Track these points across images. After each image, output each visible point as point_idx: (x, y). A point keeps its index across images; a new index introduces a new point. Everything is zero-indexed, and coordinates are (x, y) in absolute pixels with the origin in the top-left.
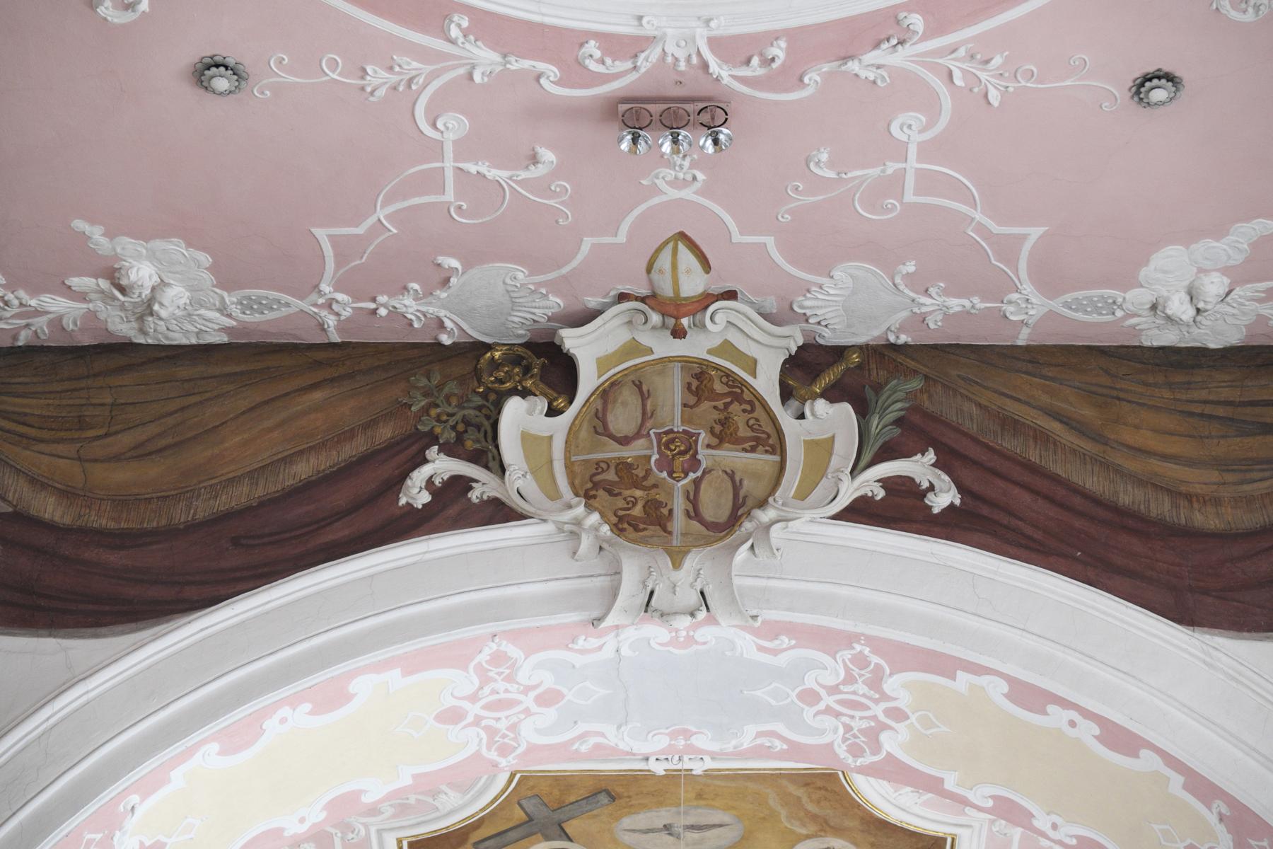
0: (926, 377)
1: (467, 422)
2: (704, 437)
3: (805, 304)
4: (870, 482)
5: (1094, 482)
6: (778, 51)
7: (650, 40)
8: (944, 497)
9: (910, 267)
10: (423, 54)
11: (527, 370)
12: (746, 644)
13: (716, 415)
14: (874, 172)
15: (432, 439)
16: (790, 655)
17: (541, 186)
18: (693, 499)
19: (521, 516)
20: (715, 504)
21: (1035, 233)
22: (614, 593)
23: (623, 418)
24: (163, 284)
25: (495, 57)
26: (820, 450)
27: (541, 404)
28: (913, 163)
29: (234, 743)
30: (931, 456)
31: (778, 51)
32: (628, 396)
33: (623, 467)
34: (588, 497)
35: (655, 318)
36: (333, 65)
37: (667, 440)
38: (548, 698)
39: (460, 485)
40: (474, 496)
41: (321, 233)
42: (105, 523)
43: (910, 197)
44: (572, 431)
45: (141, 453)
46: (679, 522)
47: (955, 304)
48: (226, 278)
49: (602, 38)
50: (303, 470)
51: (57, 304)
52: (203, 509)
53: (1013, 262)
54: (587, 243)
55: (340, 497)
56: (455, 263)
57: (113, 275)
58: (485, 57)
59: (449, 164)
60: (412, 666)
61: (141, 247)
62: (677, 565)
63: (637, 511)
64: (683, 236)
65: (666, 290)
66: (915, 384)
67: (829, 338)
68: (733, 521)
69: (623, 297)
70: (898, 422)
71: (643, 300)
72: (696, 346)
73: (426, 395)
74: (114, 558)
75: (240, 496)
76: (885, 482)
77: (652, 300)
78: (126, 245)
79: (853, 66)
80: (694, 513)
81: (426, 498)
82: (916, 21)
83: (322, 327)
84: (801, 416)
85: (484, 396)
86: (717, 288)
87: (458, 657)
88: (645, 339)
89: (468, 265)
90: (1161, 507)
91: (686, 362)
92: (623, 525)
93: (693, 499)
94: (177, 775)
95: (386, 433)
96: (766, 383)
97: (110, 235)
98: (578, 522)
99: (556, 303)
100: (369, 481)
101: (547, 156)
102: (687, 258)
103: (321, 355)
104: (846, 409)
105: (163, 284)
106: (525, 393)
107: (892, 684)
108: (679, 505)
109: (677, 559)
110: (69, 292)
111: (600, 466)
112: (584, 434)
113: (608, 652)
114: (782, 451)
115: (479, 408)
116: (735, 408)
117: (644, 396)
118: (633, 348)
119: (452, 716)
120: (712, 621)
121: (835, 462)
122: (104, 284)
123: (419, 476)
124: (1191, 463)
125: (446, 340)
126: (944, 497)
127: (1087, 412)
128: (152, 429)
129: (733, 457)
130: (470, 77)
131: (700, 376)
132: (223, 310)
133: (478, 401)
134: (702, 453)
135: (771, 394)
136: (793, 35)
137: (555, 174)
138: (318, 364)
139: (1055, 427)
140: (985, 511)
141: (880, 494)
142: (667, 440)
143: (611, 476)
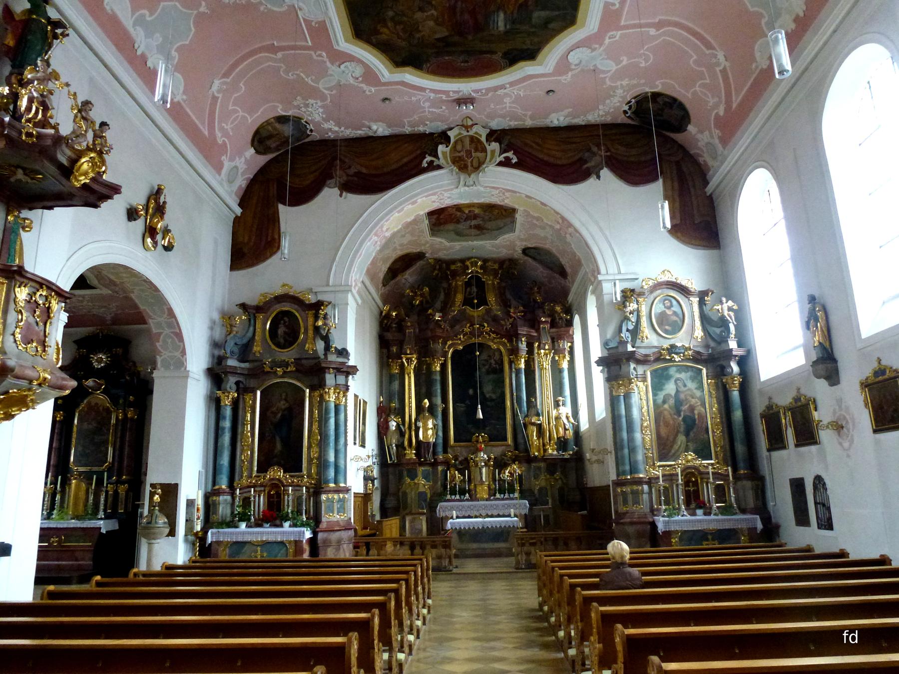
3: (489, 124)
4: (502, 158)
5: (541, 156)
6: (484, 91)
7: (461, 91)
8: (515, 160)
10: (421, 95)
12: (482, 189)
14: (501, 106)
15: (425, 153)
16: (488, 190)
17: (443, 111)
19: (442, 168)
20: (475, 164)
21: (530, 113)
22: (459, 182)
23: (459, 147)
24: (378, 128)
26: (493, 152)
27: (445, 146)
28: (508, 105)
29: (399, 212)
31: (484, 91)
32: (460, 143)
33: (460, 157)
37: (467, 151)
38: (449, 198)
39: (432, 162)
41: (405, 120)
44: (451, 150)
46: (470, 168)
47: (516, 123)
48: (389, 126)
50: (405, 160)
51: (360, 132)
57: (370, 128)
58: (432, 95)
59: (427, 110)
60: (426, 196)
65: (465, 124)
66: (509, 137)
67: (494, 129)
70: (507, 145)
72: (471, 133)
75: (394, 166)
76: (505, 157)
77: (463, 125)
80: (472, 166)
88: (462, 132)
90: (552, 160)
94: (392, 218)
95: (419, 152)
96: (483, 139)
99: (446, 127)
101: (444, 108)
102: (469, 120)
104: (498, 144)
105: (378, 128)
106: (441, 143)
108: (469, 164)
109: (469, 176)
111: (455, 157)
117: (462, 142)
118: (460, 134)
119: (434, 202)
124: (558, 151)
126: (515, 160)
127: (539, 141)
129: (479, 154)
142: (467, 151)
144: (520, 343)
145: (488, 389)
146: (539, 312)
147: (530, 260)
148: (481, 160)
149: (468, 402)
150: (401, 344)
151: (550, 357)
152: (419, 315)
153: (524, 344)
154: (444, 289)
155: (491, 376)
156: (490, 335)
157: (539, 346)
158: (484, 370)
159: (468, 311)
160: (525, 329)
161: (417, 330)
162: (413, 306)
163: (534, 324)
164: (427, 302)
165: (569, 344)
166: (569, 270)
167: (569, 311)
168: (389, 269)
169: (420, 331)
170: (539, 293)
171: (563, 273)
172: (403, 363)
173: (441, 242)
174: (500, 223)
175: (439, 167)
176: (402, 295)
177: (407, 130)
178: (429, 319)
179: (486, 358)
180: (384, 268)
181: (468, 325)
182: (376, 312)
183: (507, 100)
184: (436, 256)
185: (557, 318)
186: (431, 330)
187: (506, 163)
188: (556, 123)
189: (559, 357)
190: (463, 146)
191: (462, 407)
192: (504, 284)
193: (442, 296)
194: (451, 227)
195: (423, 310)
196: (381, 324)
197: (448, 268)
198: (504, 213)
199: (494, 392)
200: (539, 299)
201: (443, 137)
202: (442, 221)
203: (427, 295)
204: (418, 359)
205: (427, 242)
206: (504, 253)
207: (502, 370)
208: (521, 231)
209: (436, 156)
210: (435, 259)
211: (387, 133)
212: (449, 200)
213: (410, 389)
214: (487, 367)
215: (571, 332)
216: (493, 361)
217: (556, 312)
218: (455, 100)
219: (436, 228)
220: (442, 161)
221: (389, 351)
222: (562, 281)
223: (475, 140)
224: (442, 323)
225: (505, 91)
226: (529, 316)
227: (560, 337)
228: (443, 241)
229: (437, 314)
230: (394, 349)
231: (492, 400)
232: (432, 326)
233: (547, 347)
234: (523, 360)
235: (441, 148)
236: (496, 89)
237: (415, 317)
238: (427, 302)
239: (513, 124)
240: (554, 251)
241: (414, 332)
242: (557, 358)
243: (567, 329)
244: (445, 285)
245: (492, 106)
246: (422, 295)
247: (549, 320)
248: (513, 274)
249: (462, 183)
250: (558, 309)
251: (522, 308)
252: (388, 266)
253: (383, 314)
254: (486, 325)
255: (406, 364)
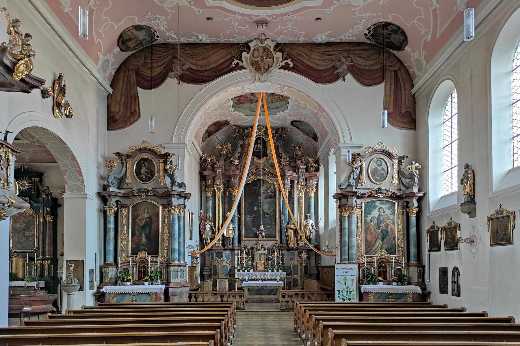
0: (290, 48)
1: (238, 54)
2: (265, 57)
4: (283, 64)
6: (274, 16)
9: (289, 36)
10: (233, 17)
11: (245, 47)
12: (269, 84)
13: (266, 54)
15: (234, 57)
18: (264, 66)
19: (245, 68)
20: (266, 67)
23: (256, 54)
25: (241, 17)
26: (278, 58)
27: (247, 53)
28: (290, 27)
30: (290, 59)
32: (256, 51)
33: (256, 61)
34: (252, 65)
35: (259, 41)
36: (223, 18)
39: (238, 64)
40: (240, 65)
42: (200, 69)
43: (289, 29)
45: (203, 59)
46: (262, 69)
47: (294, 39)
48: (210, 37)
49: (254, 15)
50: (221, 61)
51: (190, 40)
52: (210, 67)
53: (301, 36)
54: (252, 34)
55: (225, 65)
56: (236, 36)
58: (240, 17)
61: (200, 34)
62: (262, 76)
63: (258, 68)
64: (263, 33)
65: (261, 38)
66: (289, 49)
67: (279, 42)
68: (268, 69)
69: (256, 39)
70: (287, 54)
71: (258, 39)
72: (264, 45)
73: (234, 51)
74: (202, 74)
75: (214, 65)
78: (198, 34)
79: (283, 18)
81: (234, 66)
82: (291, 13)
83: (221, 41)
84: (276, 54)
85: (240, 51)
86: (267, 38)
87: (239, 86)
88: (258, 44)
89: (238, 36)
91: (263, 46)
92: (256, 69)
93: (264, 66)
95: (229, 56)
96: (272, 49)
97: (197, 33)
98: (251, 70)
100: (228, 63)
101: (247, 26)
102: (263, 35)
103: (221, 45)
104: (281, 53)
106: (245, 51)
107: (285, 88)
108: (262, 67)
109: (262, 74)
110: (192, 39)
112: (251, 56)
113: (255, 84)
114: (273, 59)
115: (240, 53)
116: (268, 53)
118: (257, 45)
120: (266, 82)
121: (279, 61)
122: (196, 38)
123: (233, 63)
125: (235, 43)
127: (308, 53)
128: (203, 56)
129: (268, 60)
130: (238, 19)
131: (264, 48)
132: (210, 40)
133: (239, 52)
134: (265, 59)
135: (272, 51)
136: (276, 15)
137: (248, 27)
138: (221, 46)
139: (304, 55)
140: (296, 67)
141: (284, 65)
143: (255, 63)
144: (286, 180)
145: (266, 207)
146: (299, 162)
147: (295, 128)
148: (270, 64)
149: (253, 214)
150: (214, 178)
151: (304, 190)
152: (225, 161)
153: (289, 181)
154: (241, 145)
155: (269, 200)
156: (268, 175)
157: (298, 183)
158: (264, 196)
159: (255, 160)
160: (290, 172)
161: (224, 170)
162: (221, 155)
163: (295, 169)
164: (230, 153)
165: (316, 182)
166: (319, 136)
167: (317, 162)
168: (206, 130)
169: (225, 171)
170: (299, 150)
171: (315, 138)
172: (214, 190)
173: (239, 115)
174: (278, 104)
175: (243, 68)
176: (214, 148)
177: (222, 40)
178: (231, 163)
179: (265, 189)
180: (204, 130)
181: (255, 168)
182: (198, 158)
183: (289, 23)
184: (236, 124)
185: (310, 166)
186: (233, 171)
187: (285, 67)
188: (320, 40)
189: (309, 190)
190: (258, 54)
191: (250, 218)
192: (278, 144)
193: (239, 150)
194: (247, 105)
195: (227, 158)
196: (201, 165)
197: (244, 132)
198: (281, 98)
199: (269, 210)
200: (299, 154)
201: (246, 46)
202: (241, 102)
203: (230, 148)
204: (224, 188)
205: (231, 115)
206: (279, 124)
207: (274, 197)
208: (291, 110)
209: (241, 60)
210: (235, 125)
211: (208, 41)
212: (249, 90)
213: (219, 206)
214: (266, 194)
215: (318, 175)
216: (269, 191)
217: (309, 162)
218: (255, 22)
219: (237, 106)
220: (244, 64)
221: (206, 183)
222: (315, 143)
223: (266, 50)
224: (239, 167)
225: (289, 17)
226: (292, 164)
227: (311, 178)
228: (241, 114)
229: (237, 161)
230: (209, 181)
231: (268, 214)
232: (233, 168)
233: (302, 184)
234: (287, 191)
235: (244, 54)
236: (283, 15)
237: (222, 162)
238: (230, 153)
239: (292, 40)
240: (311, 124)
241: (222, 172)
242: (308, 190)
243: (315, 173)
244: (241, 142)
245: (279, 27)
246: (227, 148)
247: (305, 167)
248: (284, 137)
249: (257, 79)
250: (311, 160)
251: (288, 159)
252: (206, 129)
253: (203, 159)
254: (266, 169)
255: (217, 191)
